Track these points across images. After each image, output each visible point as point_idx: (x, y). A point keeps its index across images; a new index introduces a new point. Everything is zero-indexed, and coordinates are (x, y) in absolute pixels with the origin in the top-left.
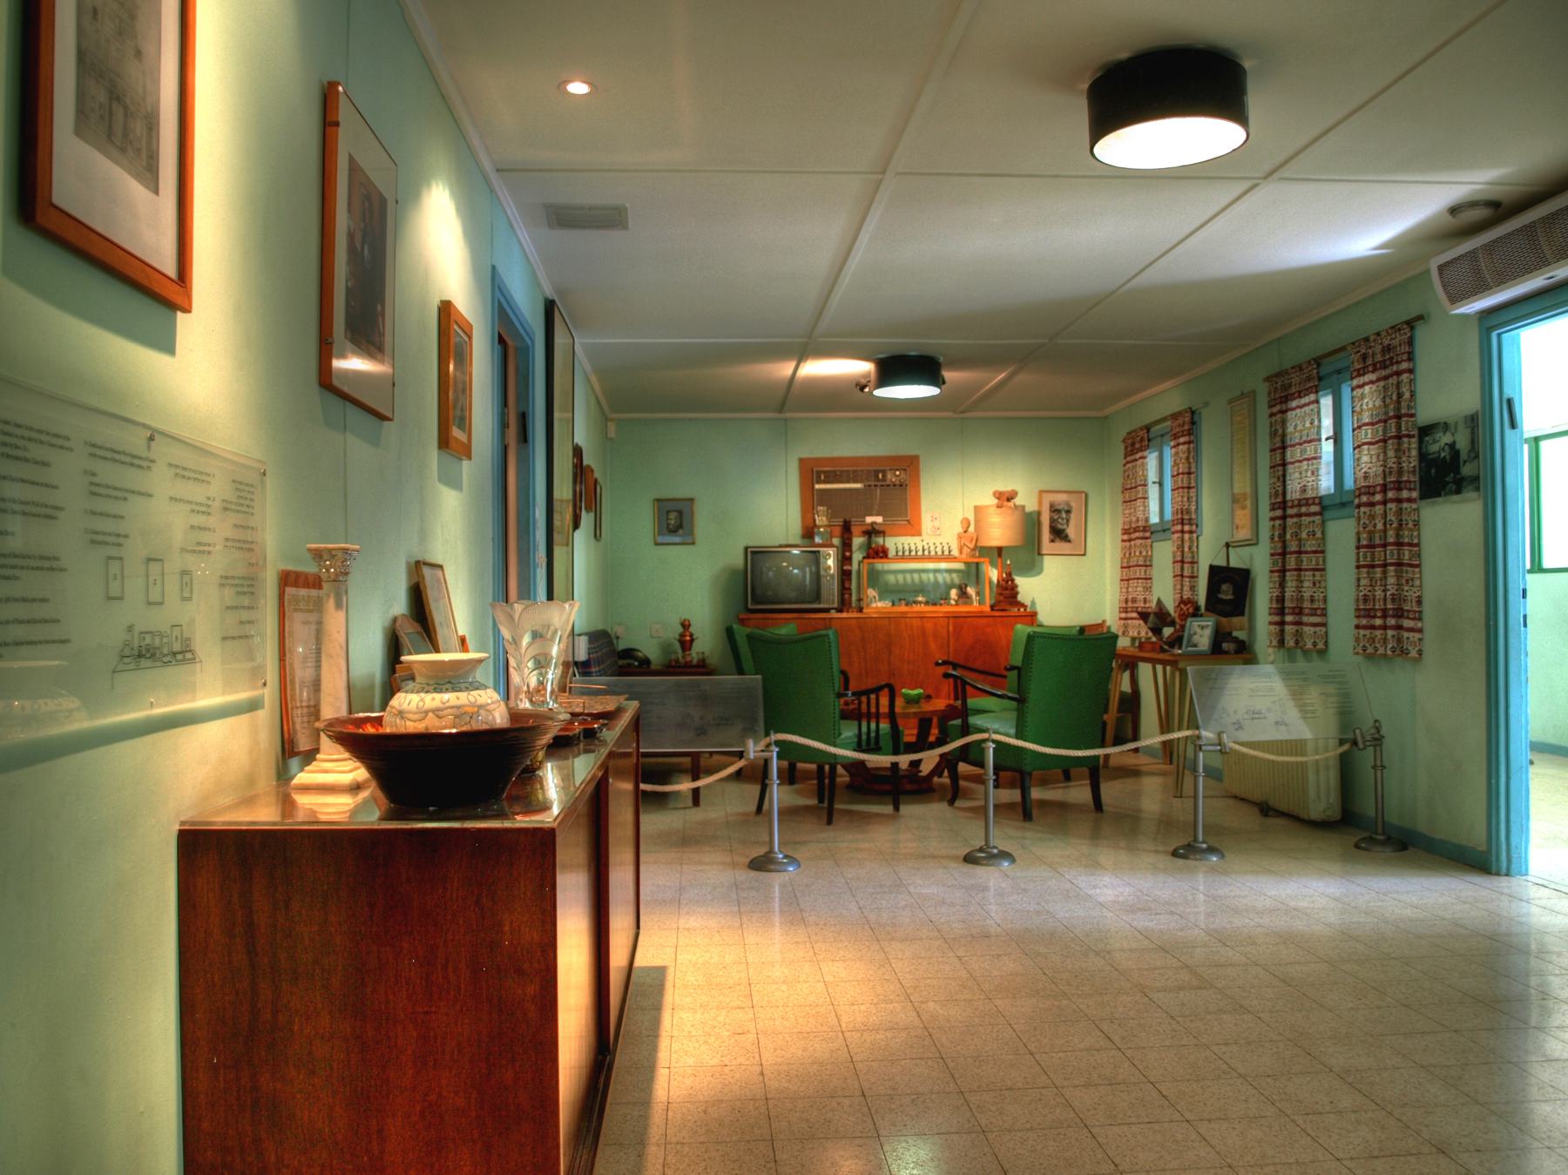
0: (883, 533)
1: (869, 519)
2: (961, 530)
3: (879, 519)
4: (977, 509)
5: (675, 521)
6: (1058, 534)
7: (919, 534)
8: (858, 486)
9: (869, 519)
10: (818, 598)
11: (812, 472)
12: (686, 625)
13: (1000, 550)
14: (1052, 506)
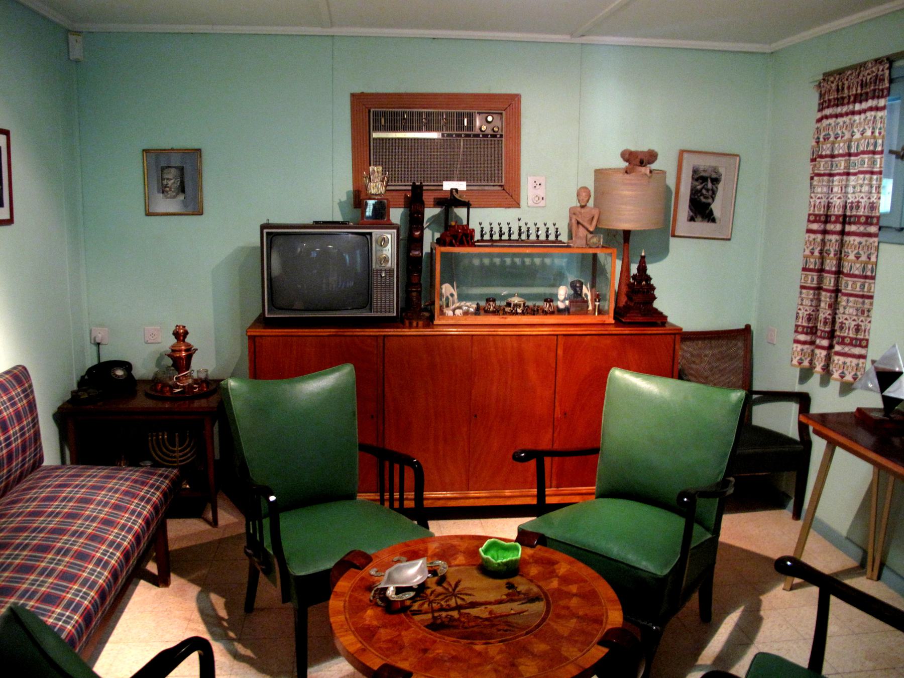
0: (467, 205)
1: (447, 186)
2: (575, 203)
3: (462, 186)
4: (600, 174)
5: (178, 176)
6: (701, 209)
7: (517, 205)
8: (434, 135)
9: (447, 186)
10: (368, 303)
11: (374, 113)
12: (180, 335)
13: (627, 234)
14: (695, 171)
